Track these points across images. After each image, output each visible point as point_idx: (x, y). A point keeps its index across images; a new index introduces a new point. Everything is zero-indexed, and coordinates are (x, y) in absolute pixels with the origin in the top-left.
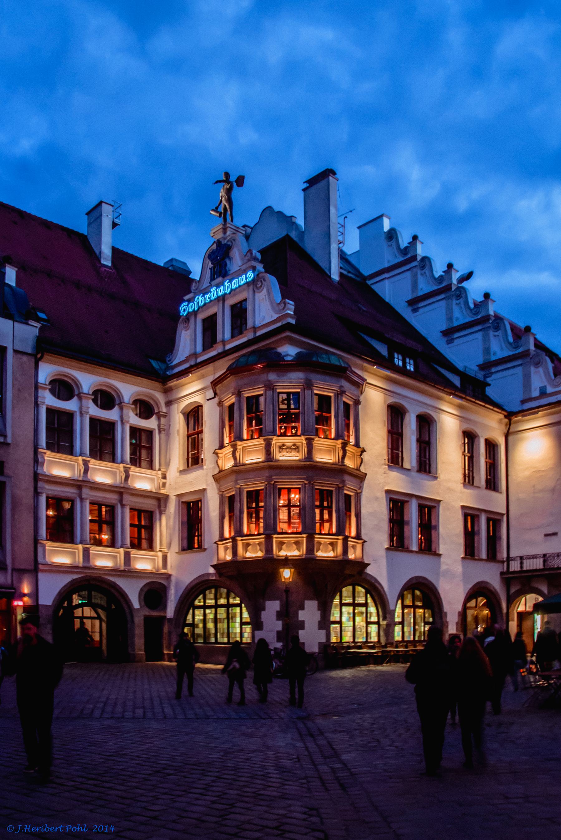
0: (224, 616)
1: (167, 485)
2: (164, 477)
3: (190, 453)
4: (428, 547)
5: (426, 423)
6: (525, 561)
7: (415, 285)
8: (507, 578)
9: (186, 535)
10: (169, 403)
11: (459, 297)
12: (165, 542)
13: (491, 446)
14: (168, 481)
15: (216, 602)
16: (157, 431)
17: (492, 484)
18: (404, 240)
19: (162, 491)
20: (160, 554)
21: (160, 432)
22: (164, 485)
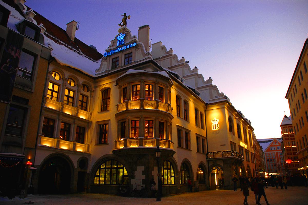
0: (115, 172)
1: (92, 118)
2: (91, 115)
3: (103, 106)
4: (188, 147)
5: (186, 103)
6: (215, 154)
7: (171, 63)
8: (209, 160)
9: (99, 138)
10: (95, 87)
11: (186, 67)
12: (89, 140)
13: (201, 114)
14: (92, 116)
15: (111, 166)
16: (90, 97)
17: (202, 127)
18: (168, 50)
19: (90, 120)
20: (87, 145)
21: (91, 97)
22: (91, 117)
